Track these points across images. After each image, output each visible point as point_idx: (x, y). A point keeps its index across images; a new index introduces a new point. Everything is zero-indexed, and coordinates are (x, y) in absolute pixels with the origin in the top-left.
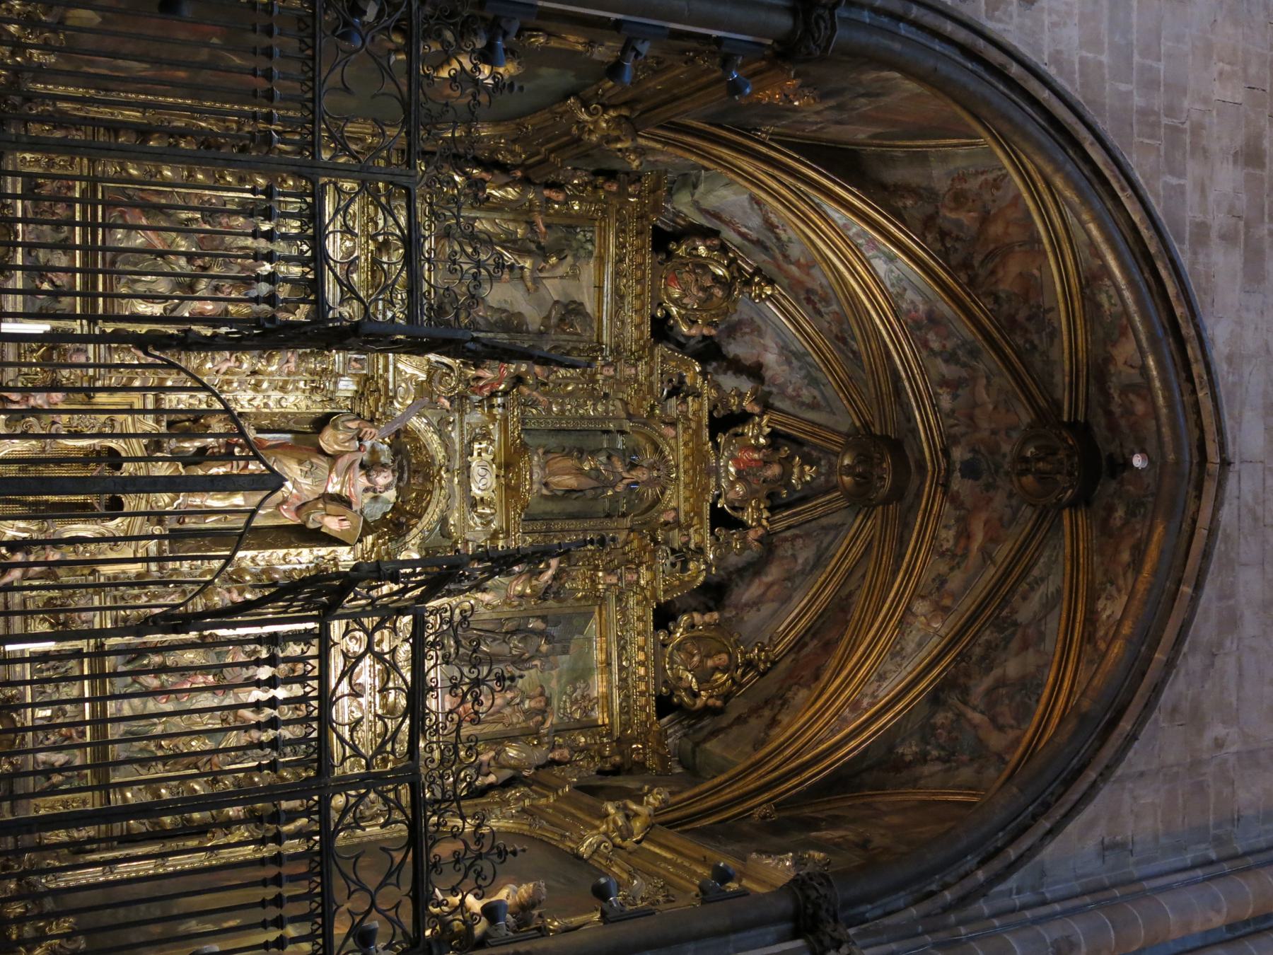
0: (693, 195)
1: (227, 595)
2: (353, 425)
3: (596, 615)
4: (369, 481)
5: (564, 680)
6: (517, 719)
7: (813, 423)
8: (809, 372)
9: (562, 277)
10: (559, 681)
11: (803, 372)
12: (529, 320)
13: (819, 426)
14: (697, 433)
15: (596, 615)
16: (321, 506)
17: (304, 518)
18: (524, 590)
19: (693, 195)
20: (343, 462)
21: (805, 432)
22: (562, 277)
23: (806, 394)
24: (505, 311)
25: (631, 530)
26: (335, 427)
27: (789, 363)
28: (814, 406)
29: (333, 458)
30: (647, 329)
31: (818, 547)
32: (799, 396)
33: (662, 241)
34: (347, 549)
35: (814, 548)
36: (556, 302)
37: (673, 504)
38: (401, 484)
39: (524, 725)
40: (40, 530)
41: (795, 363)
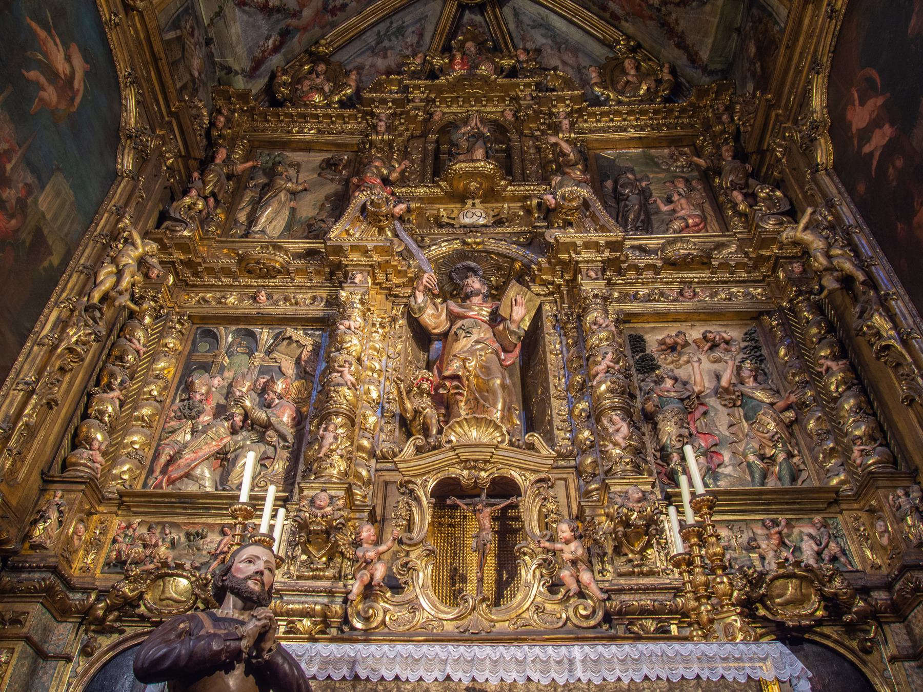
0: (237, 73)
1: (600, 375)
2: (420, 297)
3: (598, 151)
4: (477, 295)
5: (657, 170)
6: (697, 196)
7: (433, 36)
8: (394, 33)
9: (298, 172)
10: (658, 173)
11: (393, 38)
12: (332, 191)
13: (436, 30)
14: (440, 90)
15: (598, 151)
16: (501, 327)
17: (513, 339)
18: (579, 169)
19: (237, 73)
20: (456, 309)
21: (441, 39)
22: (298, 172)
23: (411, 39)
24: (323, 205)
25: (521, 134)
26: (421, 310)
27: (385, 49)
28: (421, 36)
29: (453, 318)
30: (347, 112)
31: (533, 27)
32: (412, 45)
33: (276, 103)
34: (547, 307)
35: (533, 31)
36: (319, 175)
37: (499, 114)
38: (480, 273)
39: (702, 191)
40: (531, 557)
41: (386, 43)
